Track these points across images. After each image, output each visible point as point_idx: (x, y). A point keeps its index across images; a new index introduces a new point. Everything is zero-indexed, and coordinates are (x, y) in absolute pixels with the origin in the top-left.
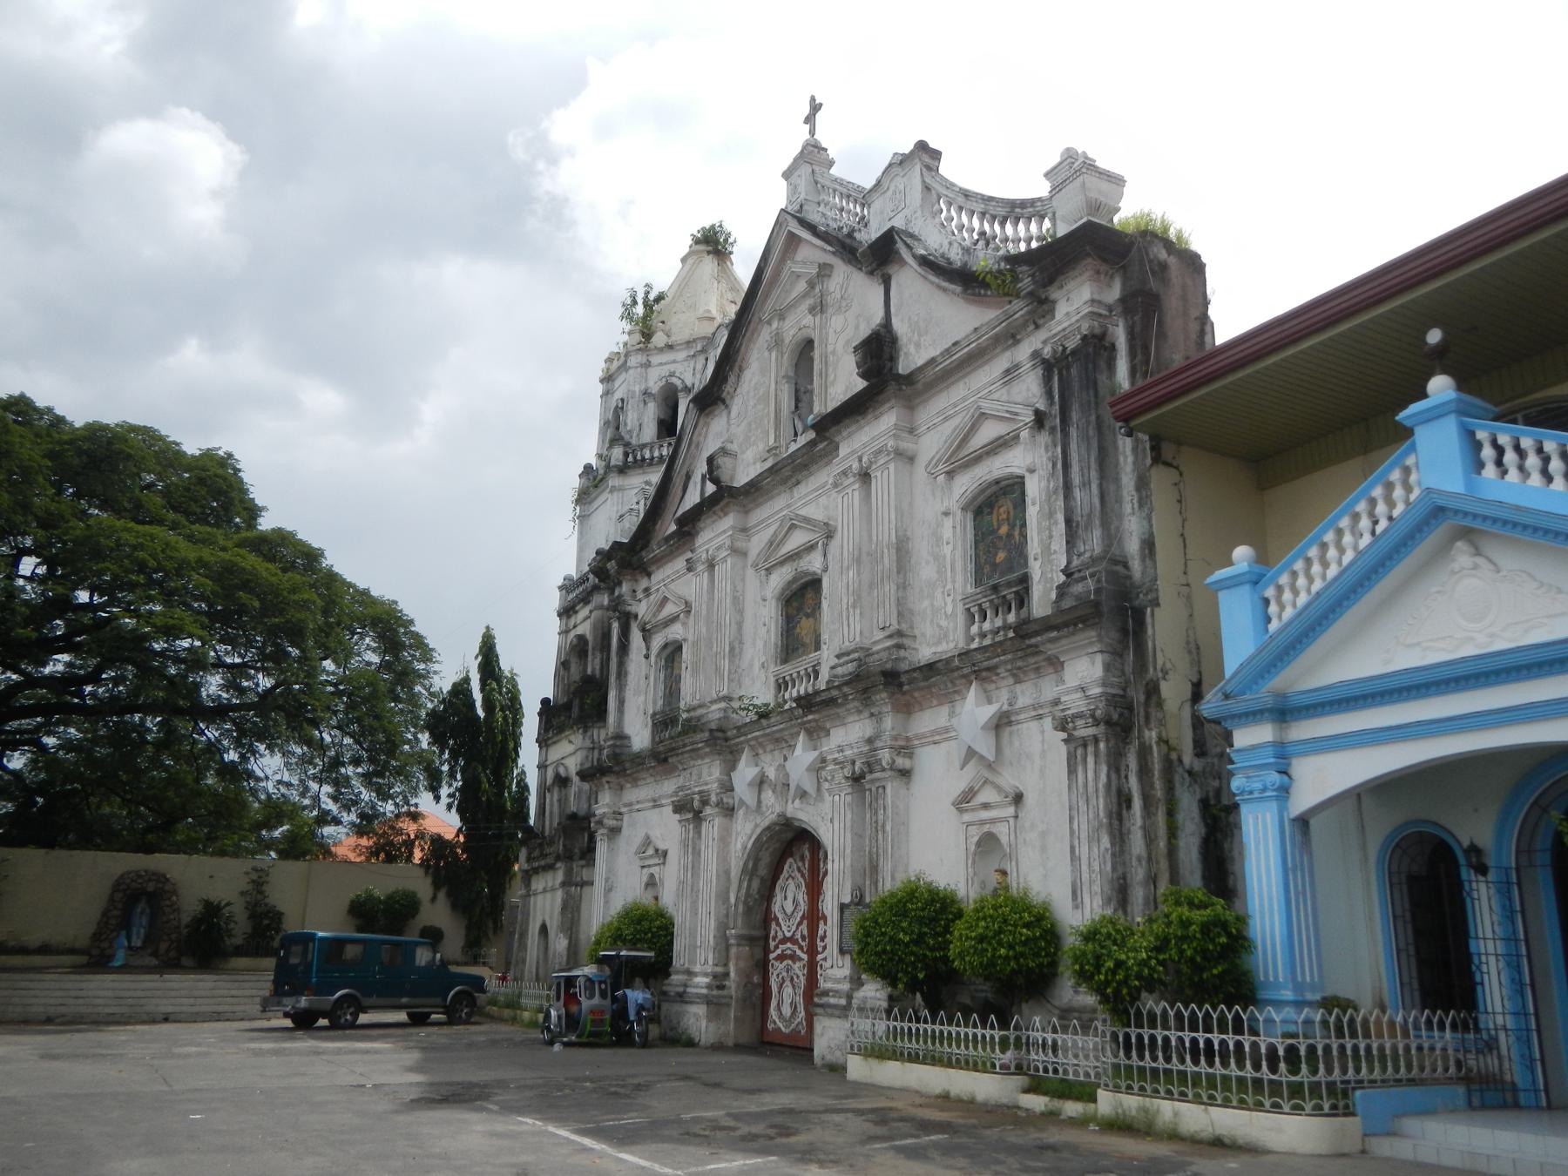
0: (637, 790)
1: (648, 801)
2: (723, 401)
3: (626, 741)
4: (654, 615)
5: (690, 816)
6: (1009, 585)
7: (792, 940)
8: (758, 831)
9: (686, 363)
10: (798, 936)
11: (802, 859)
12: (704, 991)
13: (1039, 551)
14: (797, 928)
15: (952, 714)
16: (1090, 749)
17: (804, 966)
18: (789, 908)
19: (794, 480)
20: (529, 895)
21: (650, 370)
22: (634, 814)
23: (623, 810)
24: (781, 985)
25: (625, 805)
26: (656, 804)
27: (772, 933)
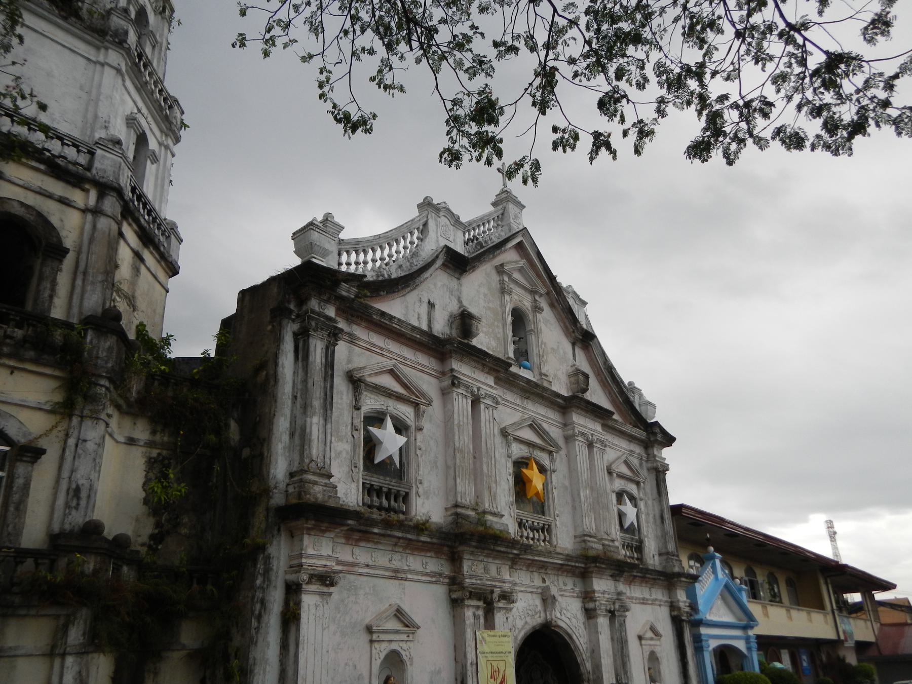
19: (528, 395)
22: (352, 577)
26: (396, 575)
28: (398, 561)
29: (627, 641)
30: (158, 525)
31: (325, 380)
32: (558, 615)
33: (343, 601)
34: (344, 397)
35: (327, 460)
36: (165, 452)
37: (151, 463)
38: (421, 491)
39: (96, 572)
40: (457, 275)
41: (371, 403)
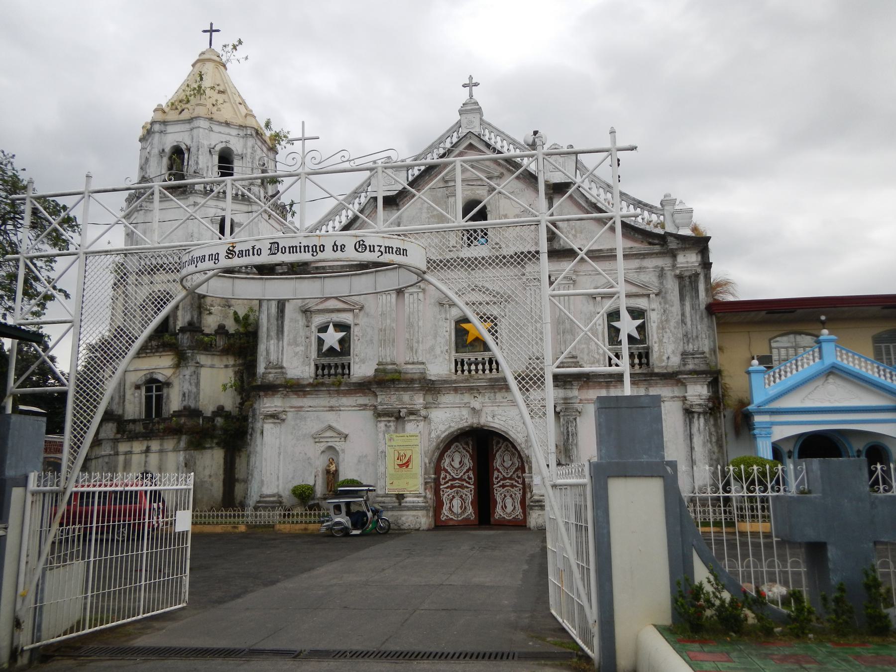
0: (305, 400)
1: (325, 407)
2: (397, 205)
3: (284, 370)
4: (317, 305)
5: (393, 419)
6: (638, 349)
7: (461, 479)
8: (452, 430)
9: (237, 139)
10: (466, 477)
11: (467, 444)
12: (424, 504)
13: (657, 340)
14: (464, 474)
15: (608, 392)
16: (701, 416)
17: (471, 491)
18: (456, 464)
20: (117, 454)
21: (211, 133)
22: (302, 413)
23: (287, 410)
24: (452, 500)
25: (292, 407)
26: (331, 409)
27: (442, 476)
28: (334, 402)
29: (575, 434)
30: (242, 398)
31: (277, 320)
32: (490, 419)
33: (297, 424)
34: (300, 323)
35: (280, 360)
36: (241, 368)
37: (236, 373)
38: (357, 360)
39: (185, 423)
40: (395, 208)
41: (318, 320)
